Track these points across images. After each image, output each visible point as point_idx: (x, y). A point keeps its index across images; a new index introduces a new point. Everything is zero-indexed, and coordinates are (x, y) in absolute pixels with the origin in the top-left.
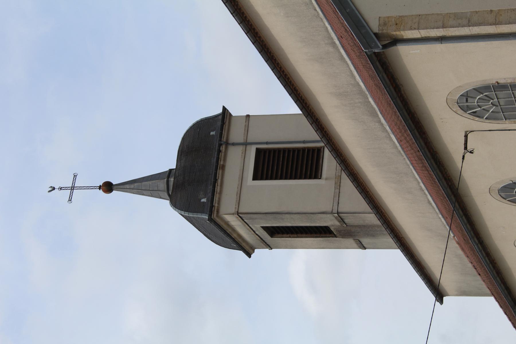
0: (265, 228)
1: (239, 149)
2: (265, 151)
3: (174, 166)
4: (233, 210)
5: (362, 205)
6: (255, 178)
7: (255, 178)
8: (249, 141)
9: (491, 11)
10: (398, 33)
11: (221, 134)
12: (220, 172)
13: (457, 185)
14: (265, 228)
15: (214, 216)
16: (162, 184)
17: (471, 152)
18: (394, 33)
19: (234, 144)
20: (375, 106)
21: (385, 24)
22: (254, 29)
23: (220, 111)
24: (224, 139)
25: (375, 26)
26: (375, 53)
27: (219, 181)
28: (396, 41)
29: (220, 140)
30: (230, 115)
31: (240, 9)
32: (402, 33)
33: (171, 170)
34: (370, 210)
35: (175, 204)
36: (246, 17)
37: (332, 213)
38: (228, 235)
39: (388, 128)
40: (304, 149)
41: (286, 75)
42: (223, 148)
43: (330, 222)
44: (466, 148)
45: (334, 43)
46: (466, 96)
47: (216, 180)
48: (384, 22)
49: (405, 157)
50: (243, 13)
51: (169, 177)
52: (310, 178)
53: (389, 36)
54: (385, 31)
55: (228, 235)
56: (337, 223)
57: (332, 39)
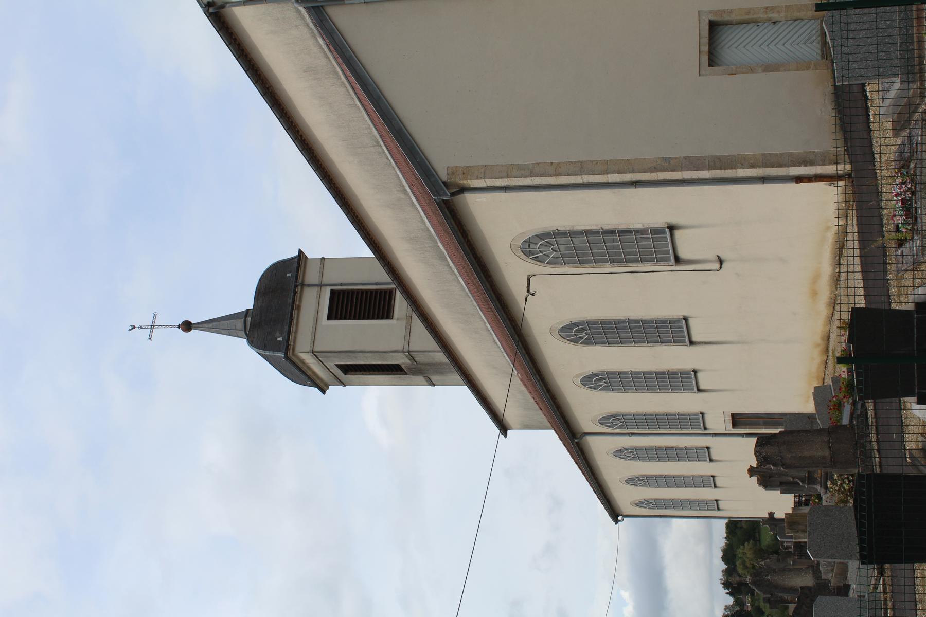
0: (339, 366)
1: (315, 291)
2: (339, 292)
3: (250, 305)
4: (308, 349)
5: (430, 343)
6: (330, 318)
7: (330, 318)
8: (324, 282)
9: (552, 163)
10: (465, 182)
11: (297, 275)
12: (295, 312)
13: (519, 324)
14: (339, 366)
15: (290, 354)
16: (240, 324)
17: (533, 295)
18: (462, 182)
19: (309, 286)
20: (444, 250)
21: (453, 173)
22: (329, 176)
23: (296, 253)
26: (443, 200)
27: (295, 321)
28: (463, 190)
29: (296, 282)
30: (306, 257)
31: (316, 157)
32: (469, 182)
33: (248, 310)
35: (252, 343)
36: (321, 164)
37: (403, 351)
38: (304, 373)
39: (456, 271)
40: (376, 291)
41: (359, 220)
42: (299, 289)
43: (401, 360)
44: (528, 291)
45: (406, 190)
46: (529, 242)
47: (291, 320)
48: (452, 172)
49: (472, 298)
53: (456, 185)
55: (304, 373)
57: (403, 186)
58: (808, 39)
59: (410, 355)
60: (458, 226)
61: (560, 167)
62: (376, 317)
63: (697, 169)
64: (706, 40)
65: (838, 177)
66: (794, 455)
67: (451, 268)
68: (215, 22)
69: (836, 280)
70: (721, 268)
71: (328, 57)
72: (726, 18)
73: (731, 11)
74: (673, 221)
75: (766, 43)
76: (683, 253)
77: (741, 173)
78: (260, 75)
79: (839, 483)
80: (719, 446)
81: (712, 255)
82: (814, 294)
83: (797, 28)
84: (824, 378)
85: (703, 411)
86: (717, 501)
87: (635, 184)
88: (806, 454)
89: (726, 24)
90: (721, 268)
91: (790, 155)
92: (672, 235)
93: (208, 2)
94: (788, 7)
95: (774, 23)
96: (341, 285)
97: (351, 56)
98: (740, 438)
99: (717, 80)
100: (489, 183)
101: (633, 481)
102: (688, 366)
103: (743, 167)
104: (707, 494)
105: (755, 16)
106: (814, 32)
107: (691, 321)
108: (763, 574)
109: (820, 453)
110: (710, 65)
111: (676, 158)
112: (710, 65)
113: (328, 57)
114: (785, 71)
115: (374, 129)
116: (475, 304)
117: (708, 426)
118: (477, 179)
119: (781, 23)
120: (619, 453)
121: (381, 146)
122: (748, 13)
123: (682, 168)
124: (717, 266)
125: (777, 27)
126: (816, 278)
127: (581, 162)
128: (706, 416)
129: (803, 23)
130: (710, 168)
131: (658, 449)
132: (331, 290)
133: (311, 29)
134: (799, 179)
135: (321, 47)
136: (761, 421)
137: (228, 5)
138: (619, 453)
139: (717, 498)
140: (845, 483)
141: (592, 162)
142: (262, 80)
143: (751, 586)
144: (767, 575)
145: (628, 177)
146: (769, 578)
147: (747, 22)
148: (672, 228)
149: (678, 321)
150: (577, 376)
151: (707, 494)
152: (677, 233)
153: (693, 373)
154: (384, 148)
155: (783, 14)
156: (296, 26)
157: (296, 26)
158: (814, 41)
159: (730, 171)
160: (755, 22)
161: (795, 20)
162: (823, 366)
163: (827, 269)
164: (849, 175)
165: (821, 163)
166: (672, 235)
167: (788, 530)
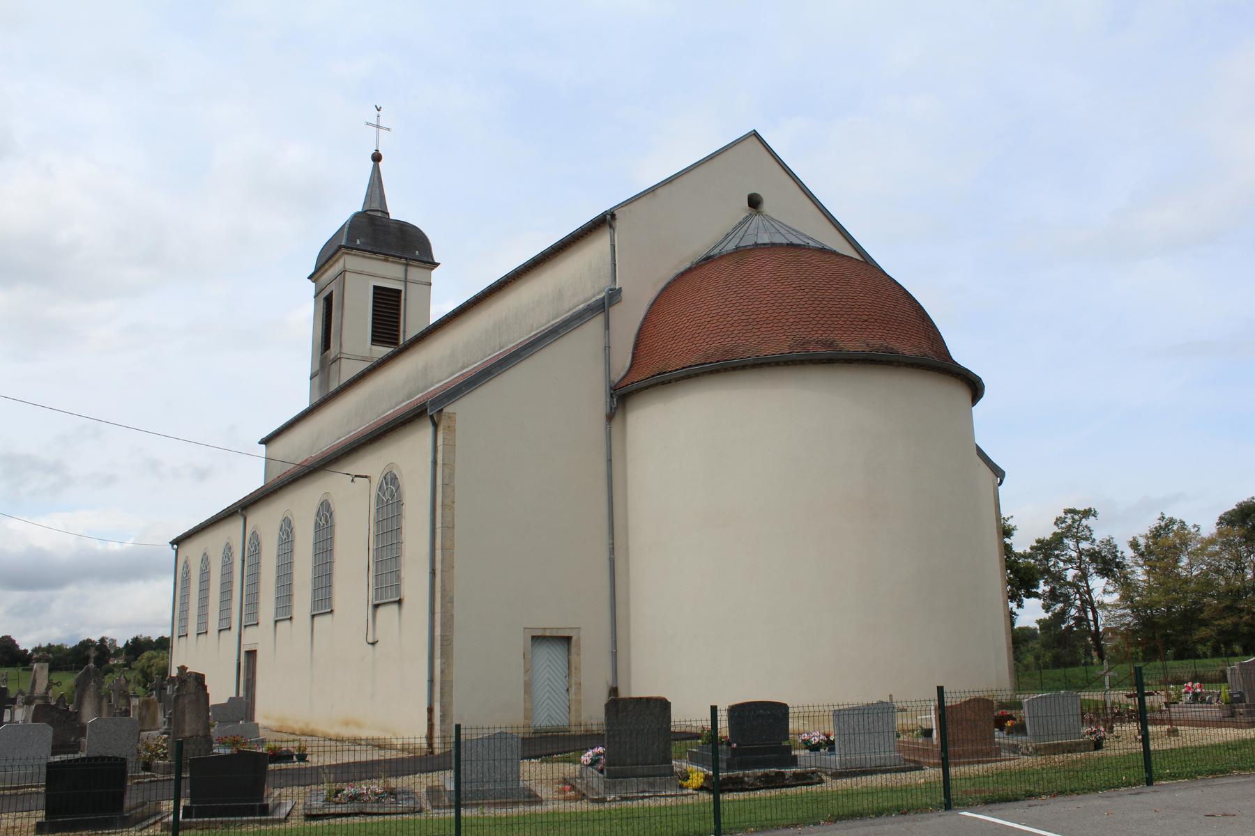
0: (331, 293)
1: (402, 276)
2: (399, 297)
3: (392, 217)
4: (348, 267)
5: (346, 376)
6: (375, 288)
7: (375, 288)
8: (409, 284)
9: (454, 502)
10: (442, 428)
11: (416, 260)
12: (382, 257)
13: (328, 469)
14: (331, 293)
15: (344, 250)
16: (376, 206)
17: (352, 481)
18: (442, 425)
19: (406, 270)
20: (415, 398)
21: (449, 418)
22: (478, 302)
23: (436, 261)
24: (411, 263)
25: (448, 409)
26: (427, 409)
27: (375, 256)
28: (436, 426)
29: (410, 259)
30: (432, 269)
31: (494, 293)
32: (441, 432)
33: (388, 214)
34: (342, 383)
35: (356, 216)
36: (488, 297)
37: (341, 353)
38: (327, 262)
39: (398, 408)
40: (398, 331)
41: (443, 326)
42: (403, 261)
43: (333, 351)
44: (356, 476)
45: (464, 369)
46: (395, 478)
47: (375, 253)
48: (451, 417)
49: (376, 420)
50: (491, 295)
51: (382, 212)
52: (373, 335)
53: (440, 420)
54: (443, 417)
55: (327, 262)
56: (332, 356)
57: (468, 366)
58: (552, 718)
59: (337, 359)
60: (408, 419)
61: (450, 509)
62: (374, 329)
63: (443, 625)
64: (555, 634)
65: (430, 745)
66: (187, 706)
67: (401, 403)
68: (599, 219)
69: (356, 742)
70: (369, 643)
71: (568, 312)
72: (573, 650)
73: (578, 654)
74: (406, 604)
75: (550, 684)
76: (381, 610)
77: (438, 662)
78: (559, 251)
79: (164, 745)
80: (231, 637)
81: (378, 637)
82: (347, 723)
83: (562, 709)
84: (282, 732)
85: (260, 625)
86: (187, 635)
87: (433, 572)
88: (187, 717)
89: (569, 650)
90: (369, 643)
91: (451, 703)
92: (394, 602)
93: (615, 215)
94: (579, 702)
95: (568, 690)
96: (405, 299)
97: (559, 334)
98: (236, 658)
99: (520, 642)
100: (440, 448)
101: (205, 560)
102: (296, 614)
103: (442, 664)
104: (193, 628)
105: (573, 674)
106: (558, 723)
107: (329, 617)
108: (96, 678)
109: (187, 728)
110: (533, 637)
111: (453, 608)
112: (533, 637)
113: (570, 310)
114: (525, 699)
115: (513, 345)
116: (371, 423)
117: (248, 629)
118: (444, 438)
119: (567, 695)
120: (228, 548)
121: (499, 350)
122: (576, 668)
123: (444, 612)
124: (371, 640)
125: (564, 692)
126: (358, 725)
127: (453, 527)
128: (255, 627)
129: (567, 715)
130: (442, 637)
131: (231, 582)
132: (401, 291)
133: (591, 299)
134: (430, 710)
135: (579, 305)
136: (250, 676)
137: (612, 231)
138: (228, 548)
139: (188, 636)
140: (165, 750)
141: (453, 537)
142: (554, 253)
143: (85, 668)
144: (95, 682)
145: (438, 566)
146: (92, 683)
147: (569, 668)
148: (400, 602)
149: (330, 605)
150: (292, 515)
151: (193, 628)
152: (396, 607)
153: (289, 617)
154: (498, 352)
155: (574, 697)
156: (594, 287)
157: (594, 287)
158: (550, 722)
159: (439, 653)
160: (569, 675)
161: (569, 707)
162: (291, 731)
163: (365, 733)
164: (432, 753)
165: (443, 728)
166: (394, 602)
167: (141, 701)
